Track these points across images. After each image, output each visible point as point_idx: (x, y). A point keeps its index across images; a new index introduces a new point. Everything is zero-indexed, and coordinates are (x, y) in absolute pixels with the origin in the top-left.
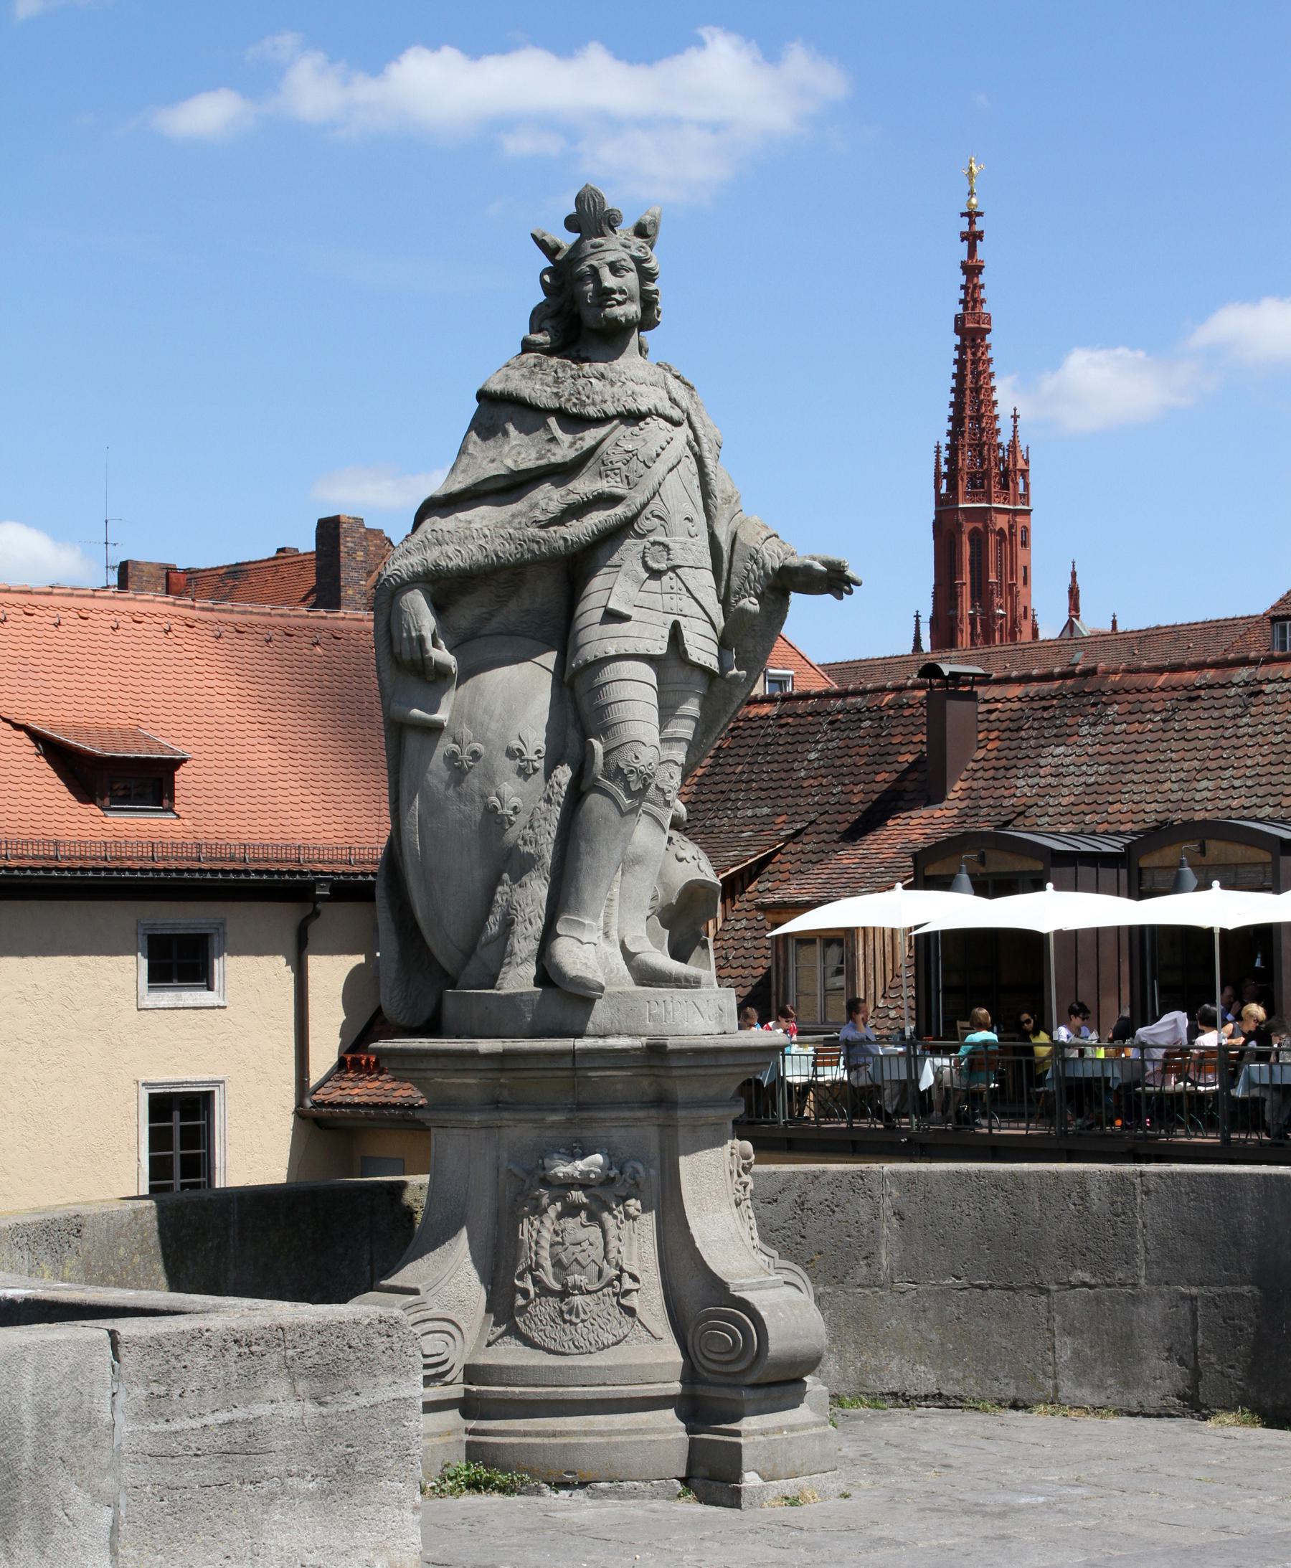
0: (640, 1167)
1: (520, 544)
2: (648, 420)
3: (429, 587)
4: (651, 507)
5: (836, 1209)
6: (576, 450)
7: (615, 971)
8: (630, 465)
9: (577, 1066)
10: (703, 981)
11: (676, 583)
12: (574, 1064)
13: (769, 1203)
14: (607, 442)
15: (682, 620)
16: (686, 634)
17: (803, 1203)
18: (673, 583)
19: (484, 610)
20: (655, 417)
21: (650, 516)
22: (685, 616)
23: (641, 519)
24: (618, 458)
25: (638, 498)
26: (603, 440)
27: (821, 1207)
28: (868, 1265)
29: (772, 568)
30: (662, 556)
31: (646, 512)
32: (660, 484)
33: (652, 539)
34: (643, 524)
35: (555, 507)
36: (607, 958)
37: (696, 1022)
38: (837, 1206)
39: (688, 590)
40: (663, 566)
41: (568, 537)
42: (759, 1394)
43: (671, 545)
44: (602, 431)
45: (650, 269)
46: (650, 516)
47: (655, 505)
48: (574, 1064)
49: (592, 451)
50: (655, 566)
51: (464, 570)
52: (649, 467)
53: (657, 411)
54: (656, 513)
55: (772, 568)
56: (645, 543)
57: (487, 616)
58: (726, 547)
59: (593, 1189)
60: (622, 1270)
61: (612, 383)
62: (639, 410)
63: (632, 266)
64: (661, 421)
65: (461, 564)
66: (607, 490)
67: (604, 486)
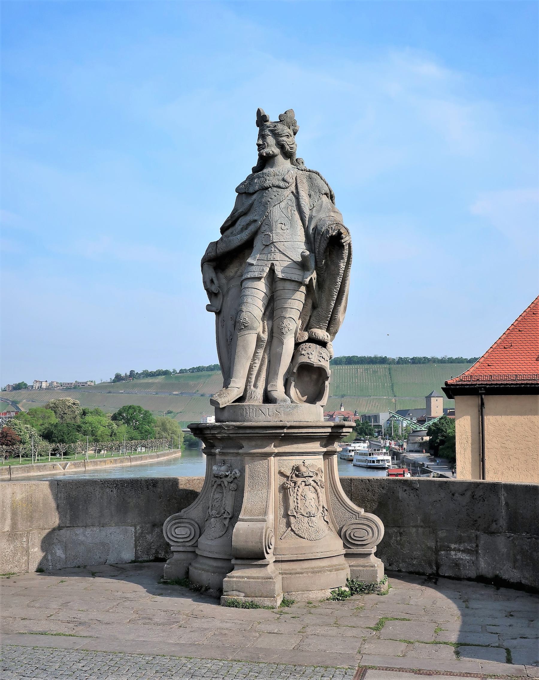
0: (237, 472)
3: (214, 264)
5: (485, 499)
7: (253, 398)
13: (462, 495)
17: (473, 496)
19: (237, 269)
22: (278, 261)
27: (480, 498)
28: (496, 524)
31: (264, 224)
34: (263, 229)
36: (251, 393)
38: (486, 498)
39: (280, 251)
40: (268, 243)
42: (239, 562)
49: (252, 205)
57: (237, 271)
59: (222, 479)
64: (275, 189)
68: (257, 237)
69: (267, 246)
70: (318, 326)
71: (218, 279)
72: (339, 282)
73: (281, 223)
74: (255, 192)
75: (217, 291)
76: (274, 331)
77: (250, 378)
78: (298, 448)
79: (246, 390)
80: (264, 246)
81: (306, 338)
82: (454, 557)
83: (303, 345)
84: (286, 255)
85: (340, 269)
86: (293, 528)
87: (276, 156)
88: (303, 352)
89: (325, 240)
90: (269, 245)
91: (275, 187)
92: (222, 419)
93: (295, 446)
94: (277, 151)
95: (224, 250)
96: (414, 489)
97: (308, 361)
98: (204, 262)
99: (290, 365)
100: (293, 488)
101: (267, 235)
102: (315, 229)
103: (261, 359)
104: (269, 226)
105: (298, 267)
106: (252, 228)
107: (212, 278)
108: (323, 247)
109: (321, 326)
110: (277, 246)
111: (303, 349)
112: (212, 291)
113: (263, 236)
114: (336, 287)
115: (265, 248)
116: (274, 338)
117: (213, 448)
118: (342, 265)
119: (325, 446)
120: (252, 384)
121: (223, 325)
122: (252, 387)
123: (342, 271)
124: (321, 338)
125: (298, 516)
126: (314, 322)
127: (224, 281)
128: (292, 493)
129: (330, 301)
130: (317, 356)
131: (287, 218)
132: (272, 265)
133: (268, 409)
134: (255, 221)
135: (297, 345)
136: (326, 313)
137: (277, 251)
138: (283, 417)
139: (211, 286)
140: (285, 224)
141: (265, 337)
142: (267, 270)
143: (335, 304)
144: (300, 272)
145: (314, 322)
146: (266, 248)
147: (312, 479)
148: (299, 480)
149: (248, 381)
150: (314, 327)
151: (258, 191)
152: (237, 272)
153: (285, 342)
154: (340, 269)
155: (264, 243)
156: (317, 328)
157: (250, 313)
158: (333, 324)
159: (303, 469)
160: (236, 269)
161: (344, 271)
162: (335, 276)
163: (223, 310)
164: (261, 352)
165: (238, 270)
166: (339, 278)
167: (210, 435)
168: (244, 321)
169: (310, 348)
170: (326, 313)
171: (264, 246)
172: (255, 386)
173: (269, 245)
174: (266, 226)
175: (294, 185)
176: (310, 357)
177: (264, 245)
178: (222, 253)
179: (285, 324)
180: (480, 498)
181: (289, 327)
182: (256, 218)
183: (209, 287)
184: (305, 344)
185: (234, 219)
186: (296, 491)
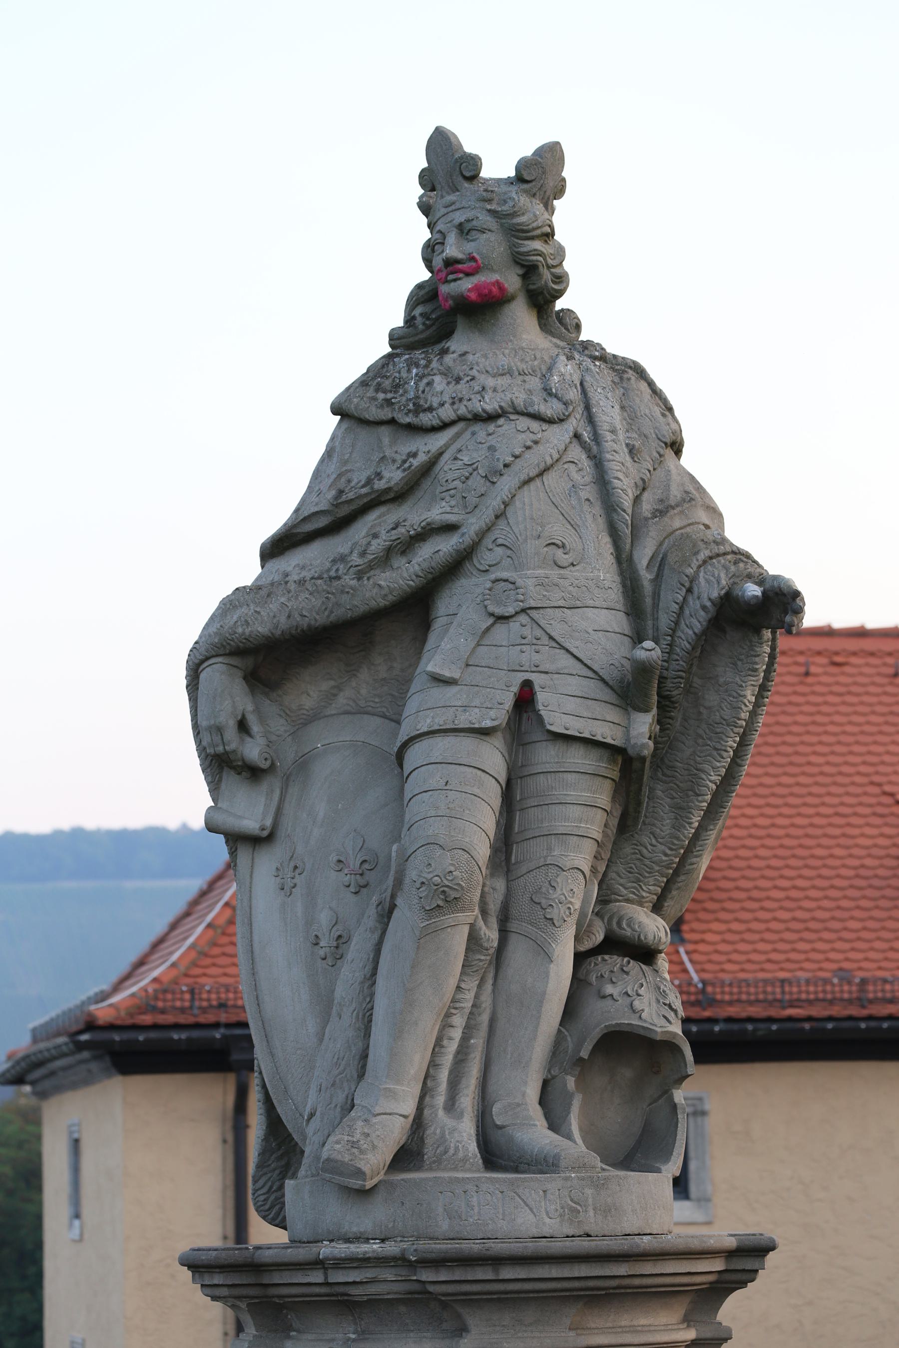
1: (327, 598)
2: (501, 421)
4: (495, 534)
6: (404, 470)
7: (452, 1151)
8: (470, 482)
9: (330, 1281)
10: (563, 1164)
12: (326, 1278)
14: (446, 456)
15: (537, 680)
16: (541, 697)
18: (527, 631)
19: (332, 683)
20: (512, 417)
22: (546, 673)
24: (457, 474)
25: (472, 526)
26: (441, 454)
29: (710, 599)
30: (508, 597)
31: (488, 542)
32: (506, 505)
33: (493, 577)
34: (485, 557)
35: (377, 546)
37: (519, 1221)
40: (510, 610)
41: (382, 583)
43: (520, 582)
44: (441, 439)
45: (518, 224)
46: (490, 547)
48: (326, 1278)
50: (499, 611)
51: (267, 638)
52: (493, 483)
53: (515, 408)
54: (500, 541)
55: (710, 599)
56: (485, 582)
58: (646, 577)
61: (458, 380)
62: (484, 410)
63: (489, 221)
64: (524, 423)
65: (260, 629)
66: (438, 517)
67: (437, 513)
70: (634, 893)
71: (262, 720)
72: (729, 749)
73: (553, 544)
74: (445, 426)
75: (268, 763)
76: (514, 912)
77: (434, 1079)
78: (633, 1330)
79: (418, 1124)
80: (491, 621)
81: (599, 937)
83: (596, 964)
84: (568, 651)
85: (743, 707)
87: (510, 299)
88: (609, 989)
89: (704, 608)
90: (512, 617)
92: (355, 1229)
93: (625, 1320)
94: (512, 281)
95: (313, 622)
97: (636, 1022)
98: (213, 656)
99: (559, 1031)
101: (503, 584)
102: (660, 563)
103: (467, 1011)
104: (509, 552)
105: (608, 695)
107: (243, 716)
108: (690, 632)
109: (644, 894)
110: (542, 623)
111: (602, 976)
112: (243, 760)
113: (489, 585)
114: (718, 764)
115: (492, 625)
116: (513, 939)
117: (289, 1337)
119: (688, 1320)
120: (440, 1100)
121: (295, 886)
122: (441, 1113)
123: (745, 715)
124: (650, 937)
126: (622, 881)
127: (279, 726)
129: (690, 813)
130: (654, 1004)
131: (569, 527)
133: (544, 1191)
134: (450, 528)
135: (580, 958)
136: (669, 852)
137: (545, 639)
138: (592, 1221)
139: (242, 741)
140: (564, 546)
141: (490, 934)
142: (508, 700)
143: (700, 823)
144: (613, 714)
145: (622, 881)
146: (498, 626)
149: (425, 1092)
150: (620, 898)
151: (453, 423)
152: (335, 695)
153: (556, 953)
154: (743, 707)
155: (491, 608)
156: (628, 901)
157: (466, 856)
158: (679, 888)
160: (326, 685)
161: (750, 712)
162: (718, 730)
163: (281, 833)
164: (471, 985)
165: (339, 688)
166: (732, 735)
167: (323, 1290)
168: (447, 883)
169: (627, 973)
170: (669, 852)
171: (491, 621)
172: (451, 1105)
173: (512, 617)
174: (500, 551)
175: (580, 409)
176: (637, 1004)
177: (492, 615)
178: (303, 630)
179: (558, 890)
181: (571, 903)
182: (452, 518)
183: (233, 746)
184: (604, 960)
185: (345, 511)
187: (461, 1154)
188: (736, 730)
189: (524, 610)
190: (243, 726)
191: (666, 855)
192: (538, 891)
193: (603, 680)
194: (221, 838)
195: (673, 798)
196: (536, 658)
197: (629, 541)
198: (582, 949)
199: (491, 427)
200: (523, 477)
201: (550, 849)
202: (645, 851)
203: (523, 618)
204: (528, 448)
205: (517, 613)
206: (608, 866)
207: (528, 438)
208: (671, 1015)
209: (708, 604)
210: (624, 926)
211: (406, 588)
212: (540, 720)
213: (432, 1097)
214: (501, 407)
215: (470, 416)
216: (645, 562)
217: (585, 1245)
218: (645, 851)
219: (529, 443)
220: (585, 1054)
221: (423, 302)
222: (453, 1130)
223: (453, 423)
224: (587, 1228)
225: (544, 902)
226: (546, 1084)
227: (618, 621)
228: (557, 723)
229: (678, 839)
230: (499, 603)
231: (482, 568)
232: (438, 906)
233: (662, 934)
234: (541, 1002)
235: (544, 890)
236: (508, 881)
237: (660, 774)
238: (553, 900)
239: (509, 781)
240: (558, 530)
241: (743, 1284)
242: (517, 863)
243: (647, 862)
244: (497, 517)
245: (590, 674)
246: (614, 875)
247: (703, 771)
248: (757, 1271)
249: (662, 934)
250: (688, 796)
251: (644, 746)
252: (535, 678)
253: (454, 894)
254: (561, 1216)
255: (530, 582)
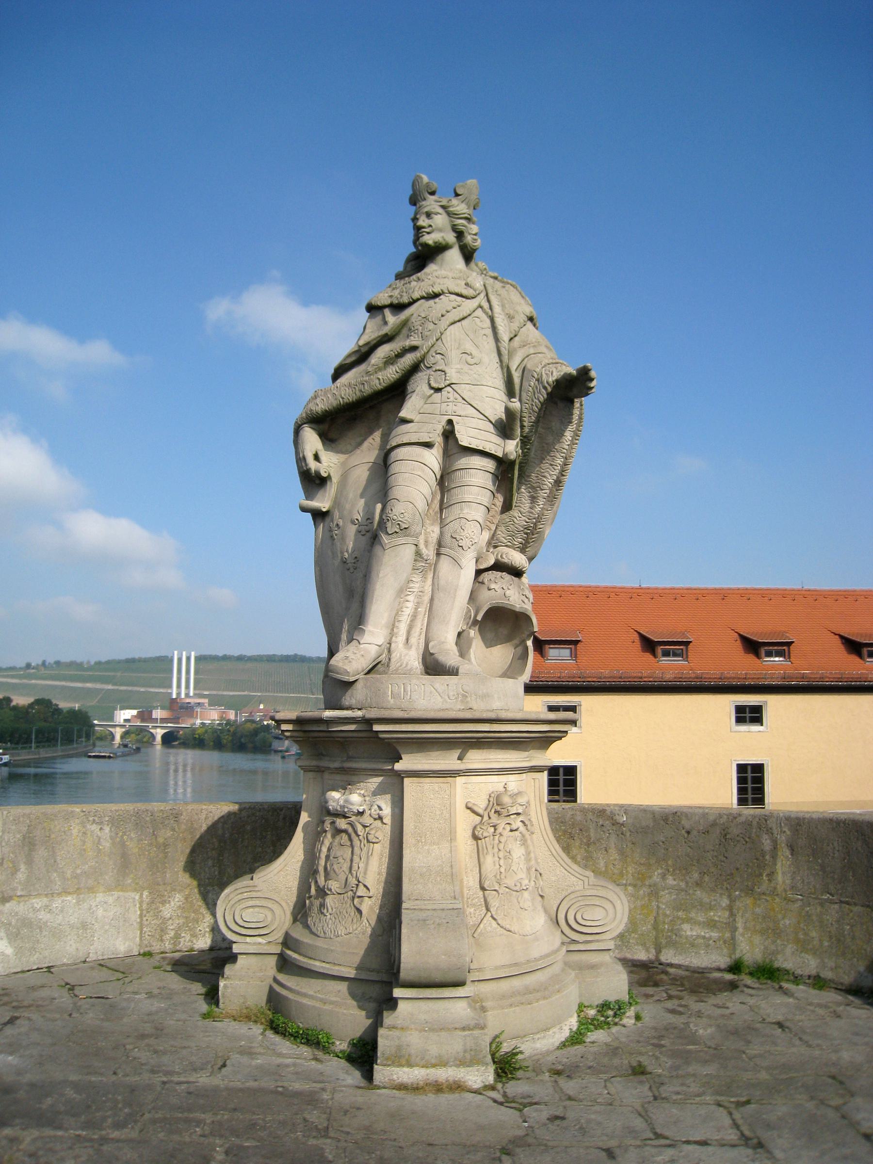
2: (442, 297)
4: (436, 348)
7: (404, 665)
11: (452, 395)
15: (455, 419)
17: (726, 835)
19: (362, 438)
21: (434, 354)
23: (429, 357)
31: (432, 352)
32: (442, 334)
33: (434, 369)
34: (430, 360)
39: (463, 399)
41: (380, 377)
47: (439, 347)
49: (405, 323)
54: (438, 352)
60: (359, 882)
64: (453, 297)
68: (417, 375)
69: (438, 390)
82: (689, 933)
86: (494, 913)
91: (450, 293)
94: (451, 238)
96: (618, 823)
100: (492, 837)
104: (443, 357)
106: (409, 359)
118: (568, 435)
125: (502, 890)
128: (490, 847)
132: (450, 422)
134: (414, 348)
135: (479, 572)
140: (471, 355)
147: (521, 818)
148: (502, 823)
151: (418, 300)
159: (506, 800)
171: (432, 391)
177: (432, 388)
180: (738, 838)
186: (496, 841)
187: (409, 667)
188: (562, 455)
189: (449, 385)
190: (317, 458)
191: (527, 522)
192: (455, 532)
193: (491, 422)
194: (309, 515)
195: (530, 492)
196: (455, 408)
197: (507, 357)
198: (482, 567)
199: (437, 300)
200: (452, 321)
201: (462, 510)
202: (515, 520)
203: (448, 389)
204: (454, 308)
205: (446, 387)
206: (496, 528)
207: (454, 304)
208: (526, 601)
209: (547, 385)
210: (504, 556)
211: (392, 379)
212: (456, 440)
213: (396, 637)
214: (442, 290)
215: (426, 296)
216: (515, 368)
217: (468, 715)
218: (515, 520)
219: (455, 306)
220: (479, 618)
221: (411, 261)
222: (406, 655)
223: (418, 300)
224: (471, 706)
225: (458, 537)
226: (459, 634)
227: (500, 395)
228: (464, 441)
229: (532, 513)
230: (436, 381)
231: (428, 366)
232: (396, 532)
233: (524, 562)
234: (456, 590)
235: (458, 531)
236: (441, 528)
237: (523, 481)
238: (463, 536)
239: (442, 477)
240: (469, 347)
241: (560, 738)
242: (445, 518)
243: (517, 526)
244: (437, 340)
245: (485, 419)
246: (500, 532)
247: (544, 477)
248: (566, 732)
249: (524, 562)
250: (537, 490)
251: (511, 453)
252: (453, 418)
253: (404, 526)
254: (456, 698)
255: (453, 371)
